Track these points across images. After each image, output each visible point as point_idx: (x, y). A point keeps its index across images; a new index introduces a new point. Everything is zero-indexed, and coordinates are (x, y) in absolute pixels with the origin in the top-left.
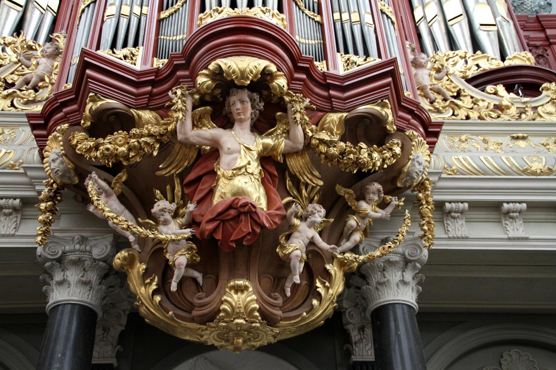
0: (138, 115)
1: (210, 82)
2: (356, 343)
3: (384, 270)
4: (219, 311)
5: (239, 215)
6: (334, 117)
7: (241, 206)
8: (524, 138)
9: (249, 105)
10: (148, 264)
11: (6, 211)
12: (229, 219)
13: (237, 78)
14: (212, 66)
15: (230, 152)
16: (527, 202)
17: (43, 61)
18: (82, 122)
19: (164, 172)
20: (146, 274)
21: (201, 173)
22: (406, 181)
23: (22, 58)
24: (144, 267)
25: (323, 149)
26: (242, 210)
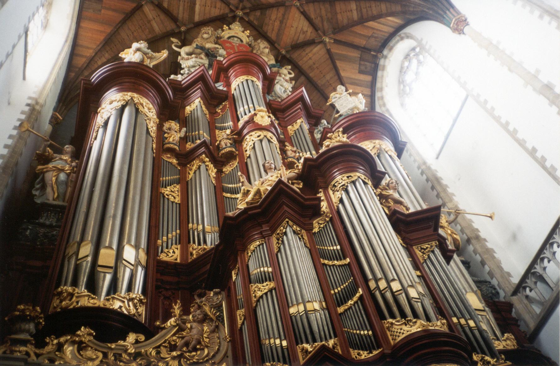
17: (194, 325)
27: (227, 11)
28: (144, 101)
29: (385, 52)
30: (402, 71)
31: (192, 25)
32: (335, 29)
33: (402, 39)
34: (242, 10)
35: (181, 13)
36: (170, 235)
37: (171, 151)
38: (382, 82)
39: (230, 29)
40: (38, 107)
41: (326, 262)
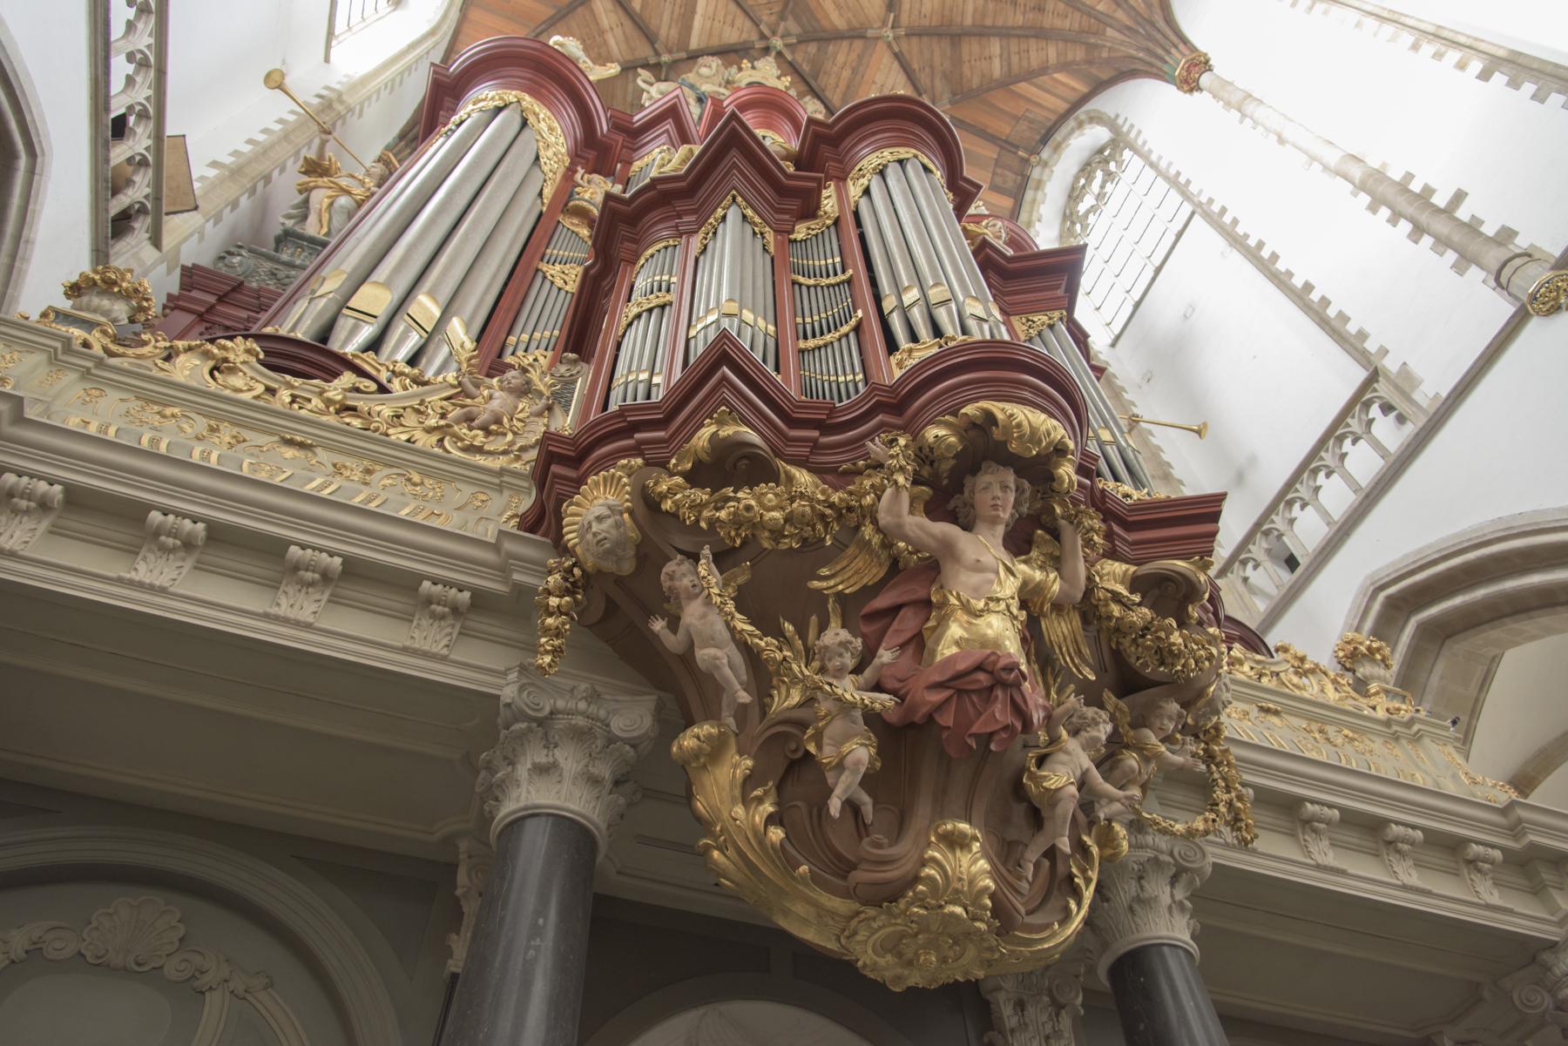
0: (787, 473)
1: (953, 439)
2: (1012, 1031)
3: (1141, 878)
4: (917, 879)
5: (991, 688)
6: (1119, 568)
7: (1004, 669)
8: (1276, 713)
9: (1012, 498)
10: (755, 758)
11: (439, 609)
12: (973, 691)
13: (1021, 437)
14: (969, 410)
15: (978, 567)
16: (1341, 809)
17: (497, 394)
18: (673, 461)
19: (824, 584)
20: (750, 781)
21: (900, 600)
22: (1204, 715)
23: (465, 380)
24: (749, 763)
25: (1116, 610)
26: (1004, 675)
27: (755, 37)
28: (543, 112)
29: (1045, 154)
30: (1074, 195)
31: (684, 55)
32: (954, 94)
33: (1080, 125)
34: (782, 37)
35: (666, 29)
36: (537, 335)
37: (581, 213)
38: (1031, 212)
39: (753, 68)
40: (339, 108)
41: (801, 279)
